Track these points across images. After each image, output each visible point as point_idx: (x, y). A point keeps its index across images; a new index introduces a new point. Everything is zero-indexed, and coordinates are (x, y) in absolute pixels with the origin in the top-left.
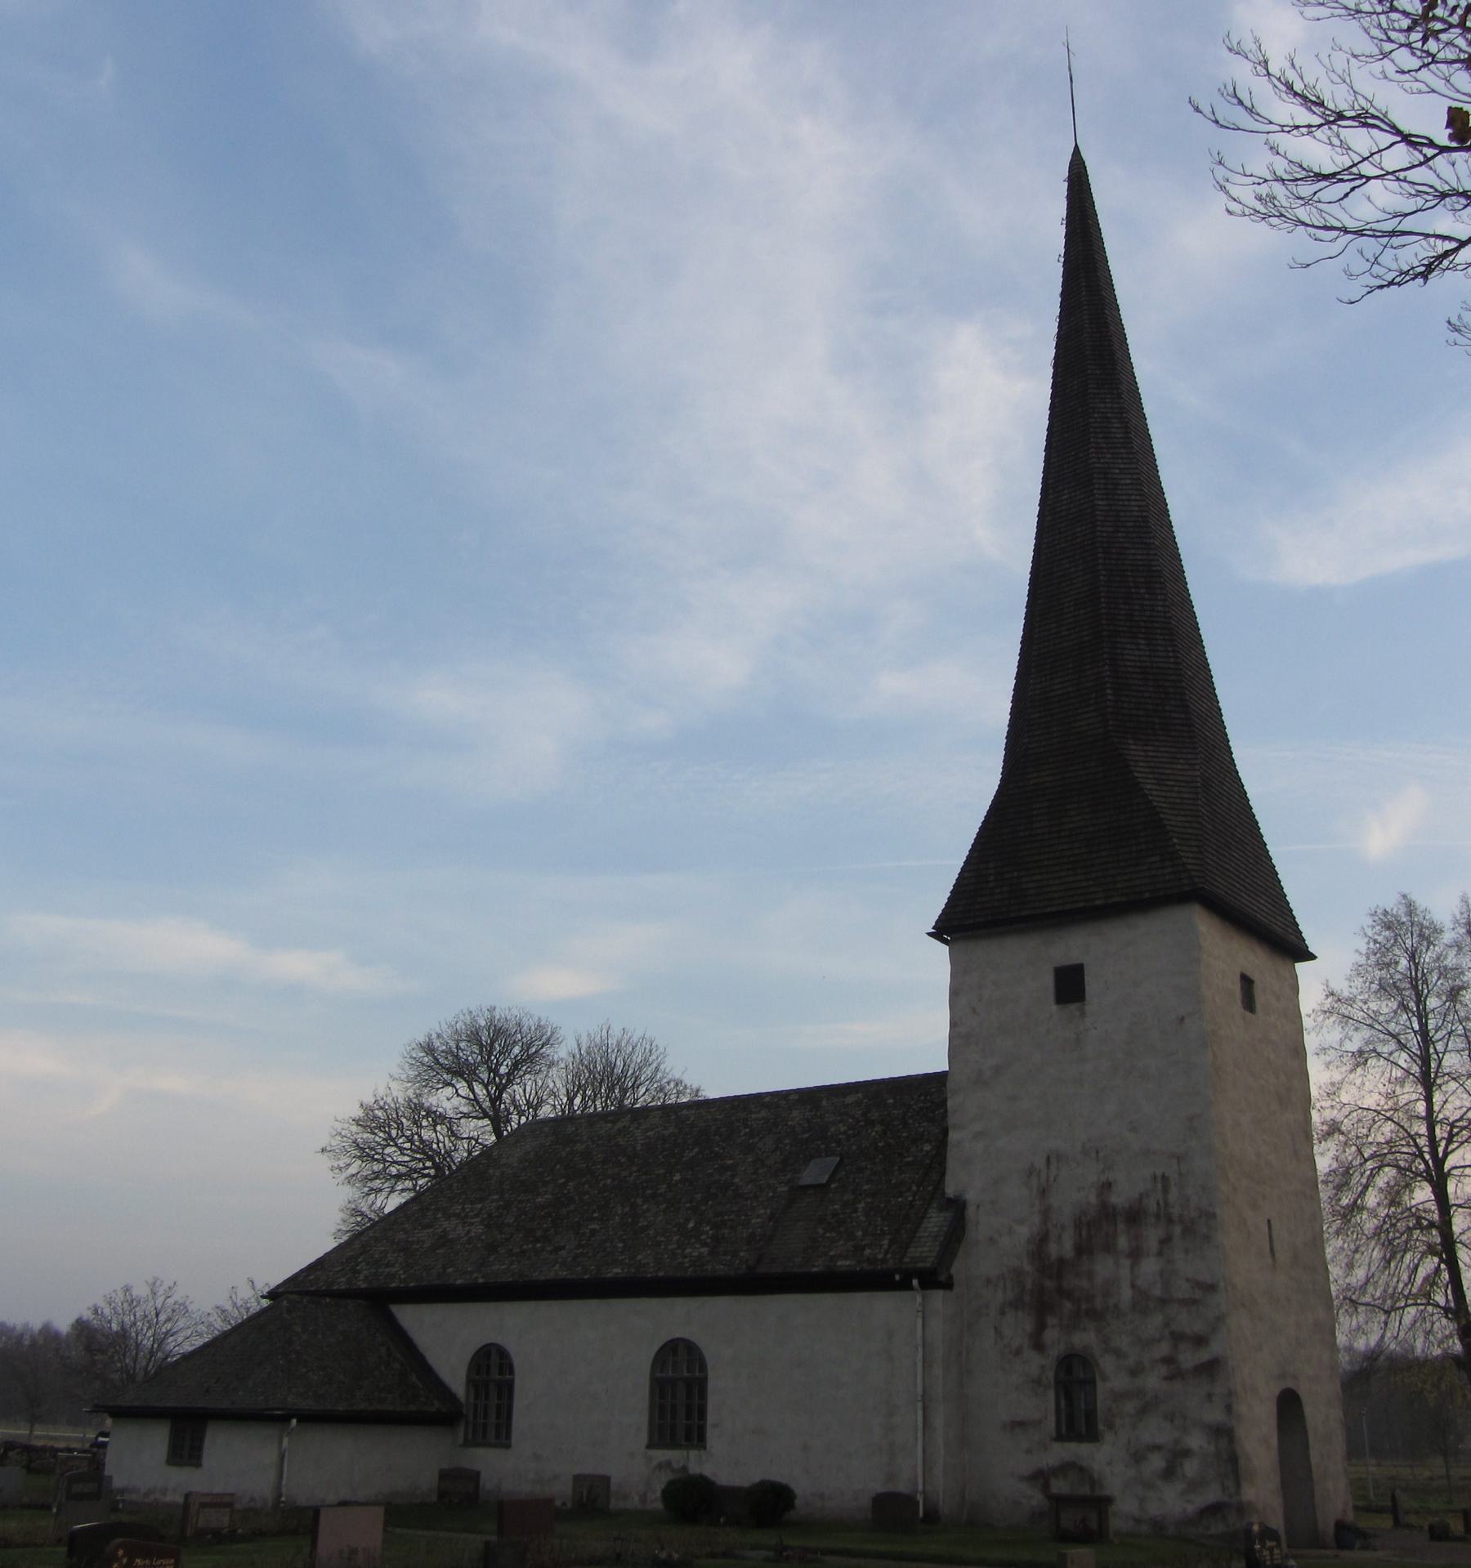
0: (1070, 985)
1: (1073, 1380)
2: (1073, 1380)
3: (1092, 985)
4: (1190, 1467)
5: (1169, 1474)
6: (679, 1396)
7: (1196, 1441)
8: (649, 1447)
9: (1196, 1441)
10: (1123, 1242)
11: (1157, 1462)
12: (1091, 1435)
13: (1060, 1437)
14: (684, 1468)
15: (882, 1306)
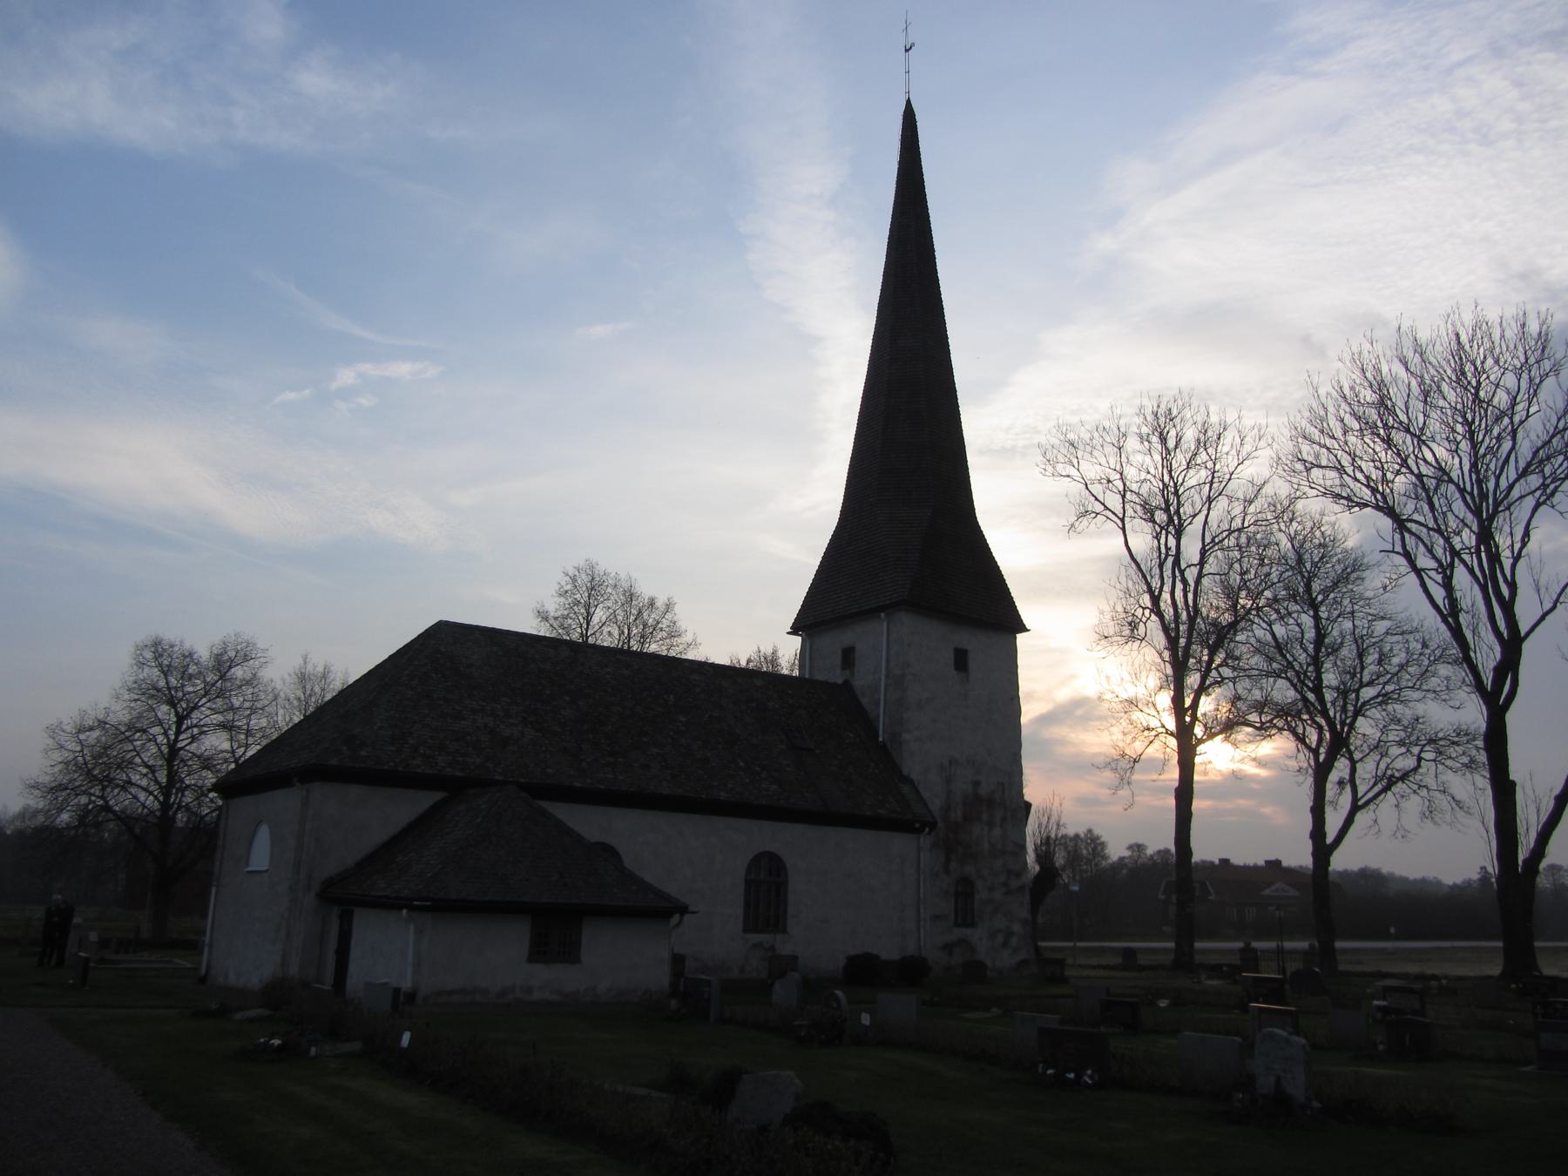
0: (961, 660)
1: (964, 893)
2: (964, 893)
3: (972, 665)
4: (1014, 941)
5: (1005, 945)
6: (766, 892)
7: (1016, 927)
8: (745, 931)
9: (1016, 927)
10: (985, 816)
11: (1000, 938)
12: (972, 925)
13: (957, 925)
14: (772, 948)
15: (899, 843)
